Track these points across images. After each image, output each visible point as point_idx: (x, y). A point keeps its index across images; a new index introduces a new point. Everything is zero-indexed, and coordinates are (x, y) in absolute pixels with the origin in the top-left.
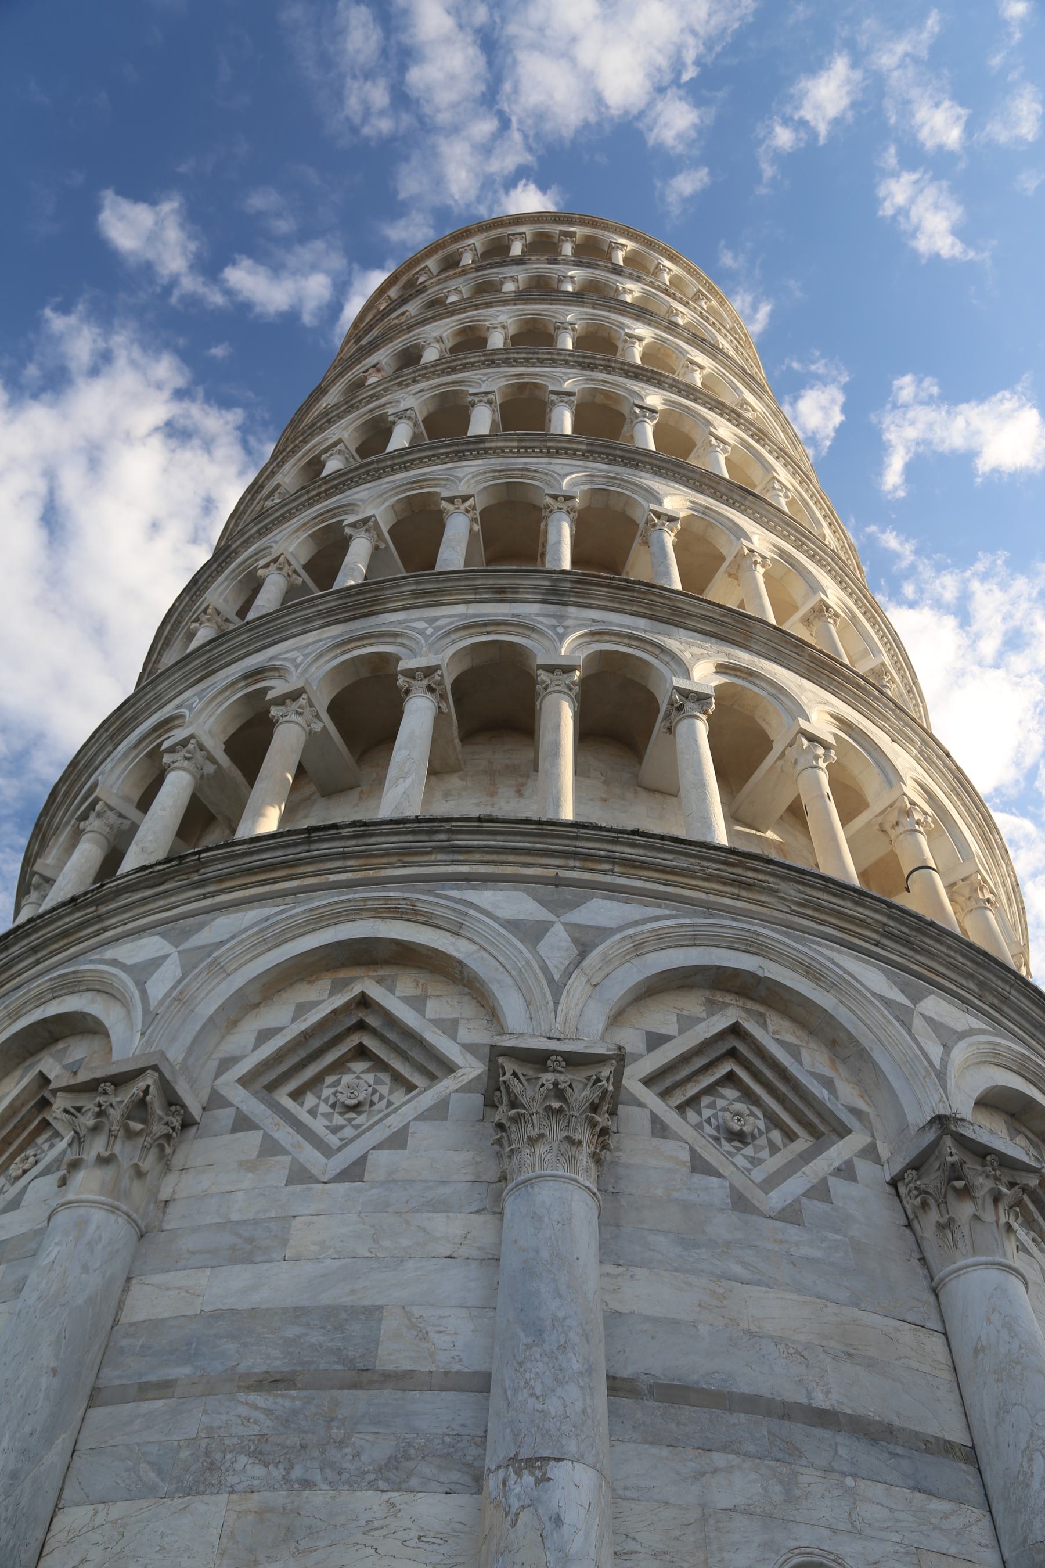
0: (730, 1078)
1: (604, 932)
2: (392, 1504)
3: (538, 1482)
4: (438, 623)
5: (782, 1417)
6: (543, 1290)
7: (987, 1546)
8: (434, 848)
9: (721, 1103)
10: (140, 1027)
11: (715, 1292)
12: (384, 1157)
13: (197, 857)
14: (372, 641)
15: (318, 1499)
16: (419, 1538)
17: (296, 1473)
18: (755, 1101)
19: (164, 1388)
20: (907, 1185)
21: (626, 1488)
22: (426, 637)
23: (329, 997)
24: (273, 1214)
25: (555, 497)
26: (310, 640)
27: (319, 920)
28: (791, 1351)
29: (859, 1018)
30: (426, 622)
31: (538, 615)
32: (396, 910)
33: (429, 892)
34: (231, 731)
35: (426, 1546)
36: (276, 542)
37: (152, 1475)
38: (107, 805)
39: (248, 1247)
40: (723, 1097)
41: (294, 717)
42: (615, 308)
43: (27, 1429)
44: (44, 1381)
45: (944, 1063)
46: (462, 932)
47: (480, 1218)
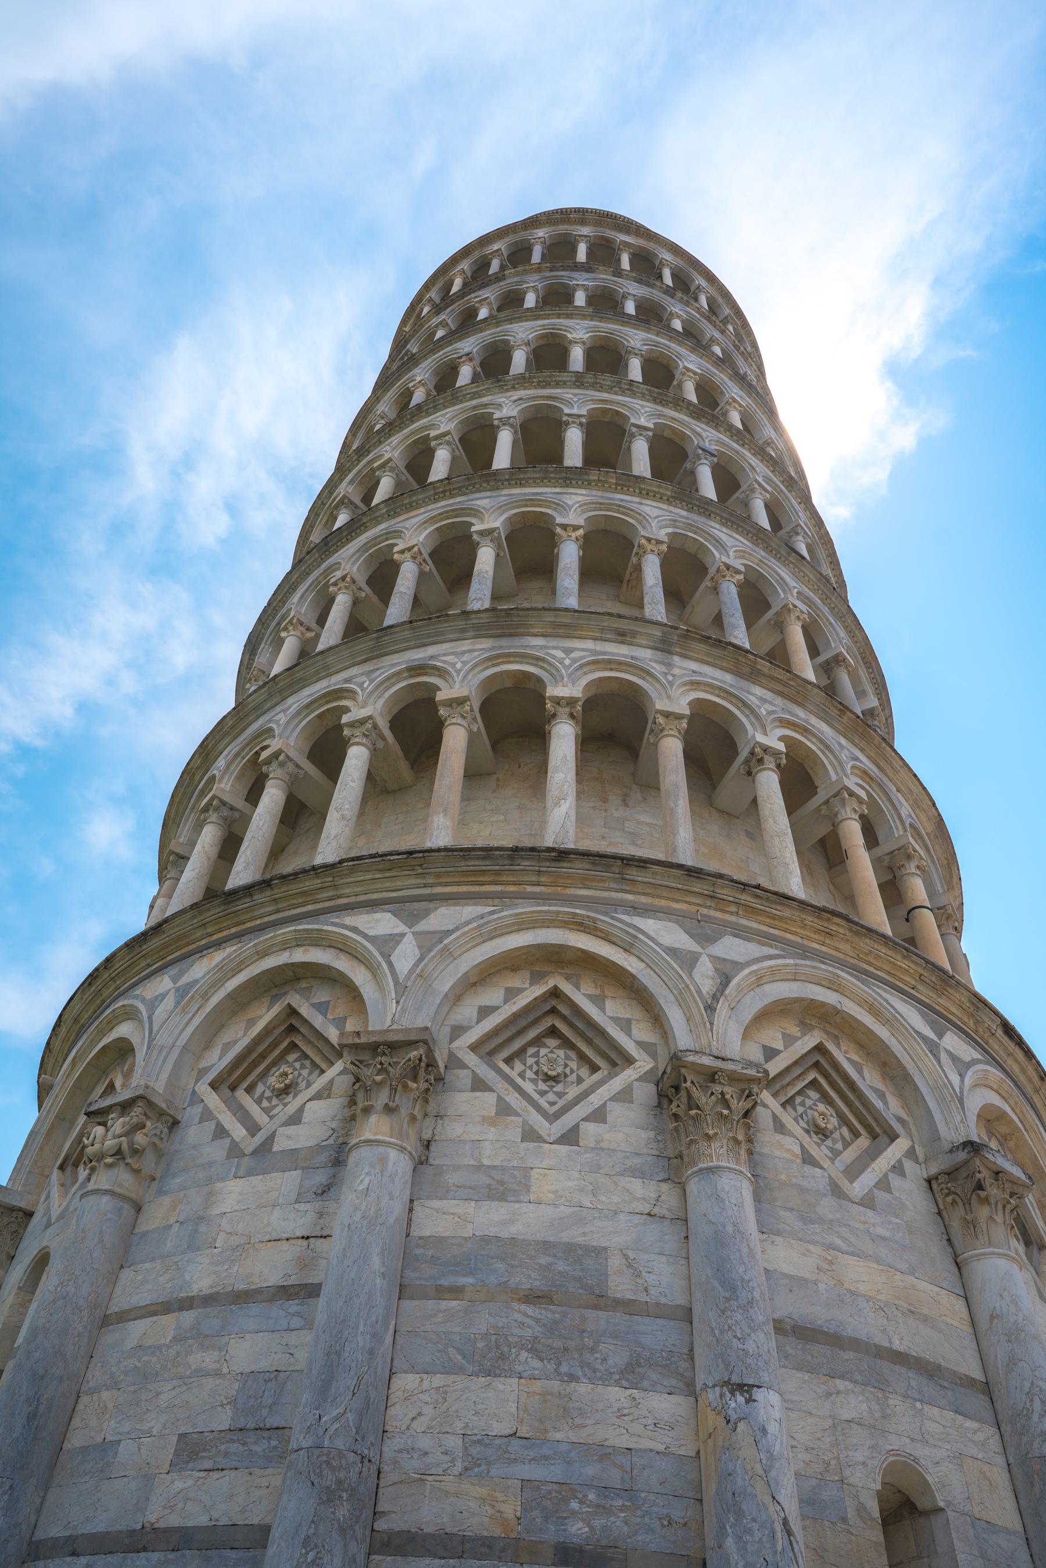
1: (739, 966)
2: (633, 1398)
4: (573, 655)
7: (998, 1453)
8: (609, 878)
10: (394, 996)
11: (826, 1259)
12: (589, 1130)
13: (421, 855)
14: (518, 659)
15: (583, 1389)
17: (564, 1368)
19: (456, 1292)
22: (564, 666)
23: (530, 986)
25: (649, 540)
26: (465, 648)
27: (522, 925)
29: (905, 1049)
30: (563, 651)
31: (651, 660)
32: (581, 924)
33: (606, 914)
34: (395, 711)
35: (660, 1430)
36: (407, 529)
37: (459, 1357)
39: (501, 1188)
40: (810, 1098)
41: (460, 721)
42: (675, 339)
43: (374, 1318)
46: (632, 950)
47: (665, 1187)
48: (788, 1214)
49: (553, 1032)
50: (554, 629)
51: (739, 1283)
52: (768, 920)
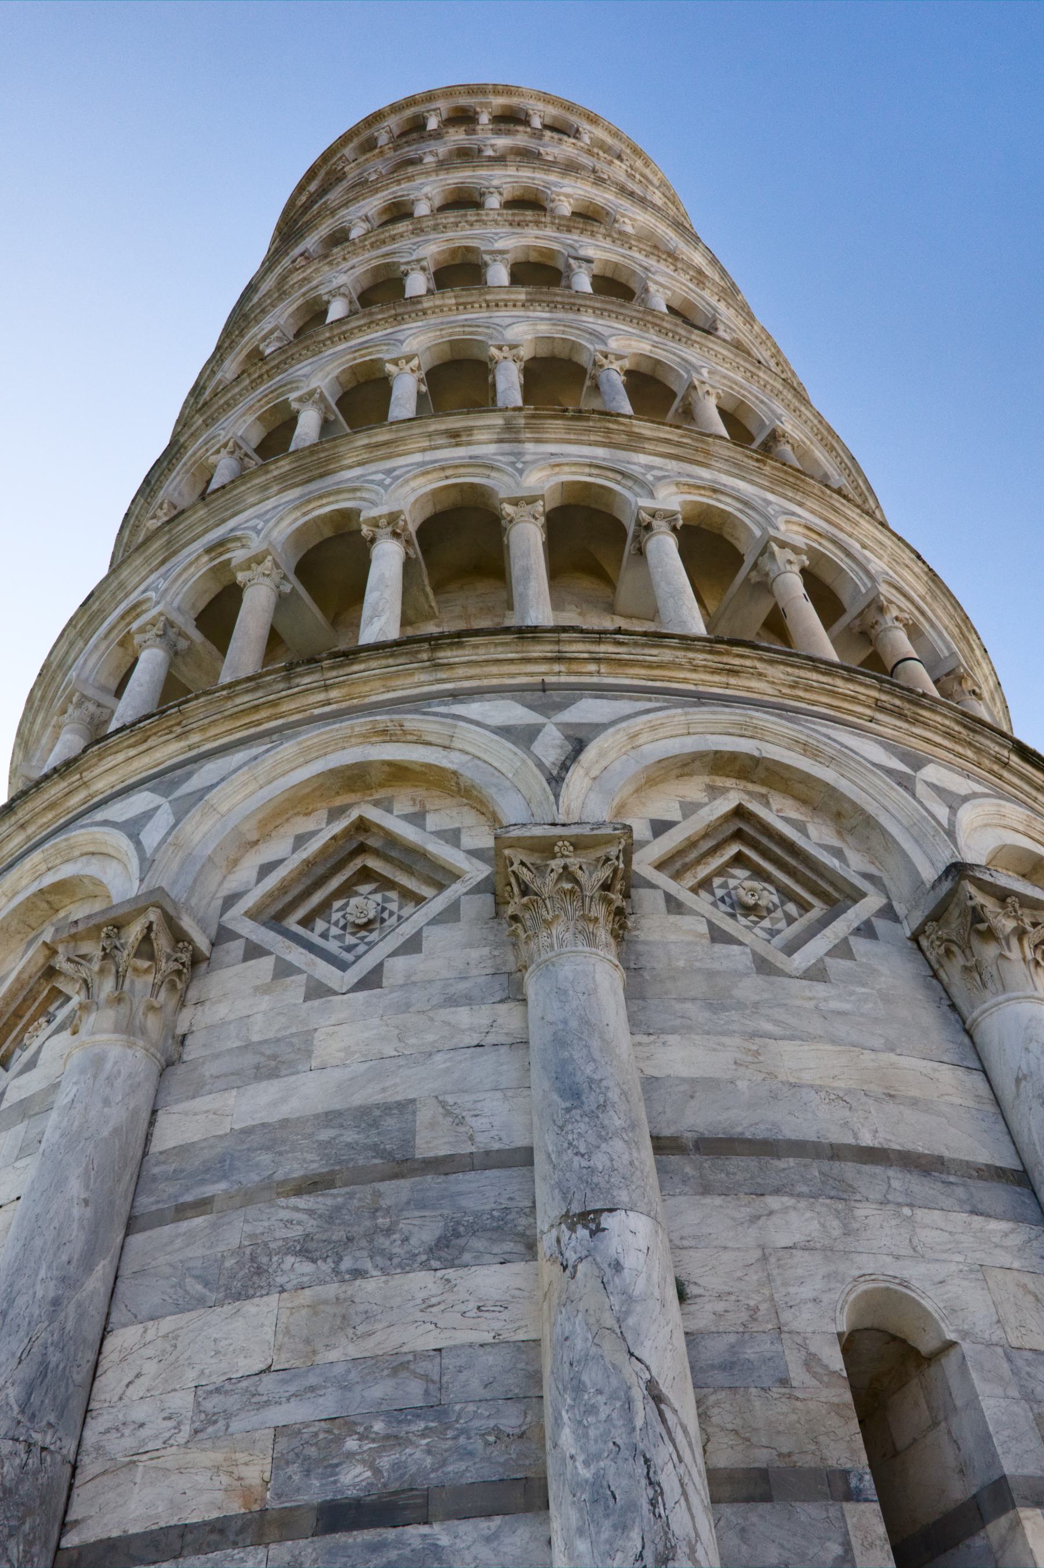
0: (739, 859)
1: (598, 728)
3: (593, 1234)
5: (832, 1158)
6: (575, 1057)
9: (732, 883)
11: (749, 1050)
13: (176, 709)
15: (371, 1286)
16: (479, 1308)
17: (346, 1264)
18: (767, 878)
19: (202, 1205)
20: (928, 937)
21: (682, 1238)
24: (294, 1030)
28: (832, 1097)
29: (862, 789)
31: (495, 454)
32: (384, 732)
34: (201, 605)
37: (199, 1287)
38: (83, 696)
39: (273, 1063)
40: (733, 877)
41: (262, 579)
43: (65, 1258)
44: (76, 1211)
45: (952, 823)
46: (453, 745)
47: (503, 1008)
48: (688, 1005)
49: (366, 875)
50: (371, 452)
51: (585, 1086)
52: (643, 672)
